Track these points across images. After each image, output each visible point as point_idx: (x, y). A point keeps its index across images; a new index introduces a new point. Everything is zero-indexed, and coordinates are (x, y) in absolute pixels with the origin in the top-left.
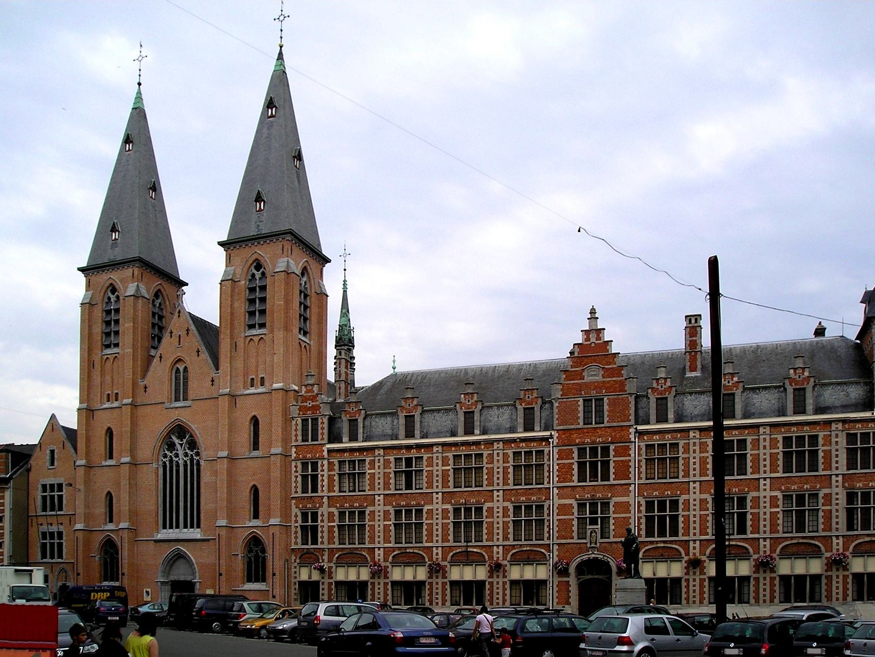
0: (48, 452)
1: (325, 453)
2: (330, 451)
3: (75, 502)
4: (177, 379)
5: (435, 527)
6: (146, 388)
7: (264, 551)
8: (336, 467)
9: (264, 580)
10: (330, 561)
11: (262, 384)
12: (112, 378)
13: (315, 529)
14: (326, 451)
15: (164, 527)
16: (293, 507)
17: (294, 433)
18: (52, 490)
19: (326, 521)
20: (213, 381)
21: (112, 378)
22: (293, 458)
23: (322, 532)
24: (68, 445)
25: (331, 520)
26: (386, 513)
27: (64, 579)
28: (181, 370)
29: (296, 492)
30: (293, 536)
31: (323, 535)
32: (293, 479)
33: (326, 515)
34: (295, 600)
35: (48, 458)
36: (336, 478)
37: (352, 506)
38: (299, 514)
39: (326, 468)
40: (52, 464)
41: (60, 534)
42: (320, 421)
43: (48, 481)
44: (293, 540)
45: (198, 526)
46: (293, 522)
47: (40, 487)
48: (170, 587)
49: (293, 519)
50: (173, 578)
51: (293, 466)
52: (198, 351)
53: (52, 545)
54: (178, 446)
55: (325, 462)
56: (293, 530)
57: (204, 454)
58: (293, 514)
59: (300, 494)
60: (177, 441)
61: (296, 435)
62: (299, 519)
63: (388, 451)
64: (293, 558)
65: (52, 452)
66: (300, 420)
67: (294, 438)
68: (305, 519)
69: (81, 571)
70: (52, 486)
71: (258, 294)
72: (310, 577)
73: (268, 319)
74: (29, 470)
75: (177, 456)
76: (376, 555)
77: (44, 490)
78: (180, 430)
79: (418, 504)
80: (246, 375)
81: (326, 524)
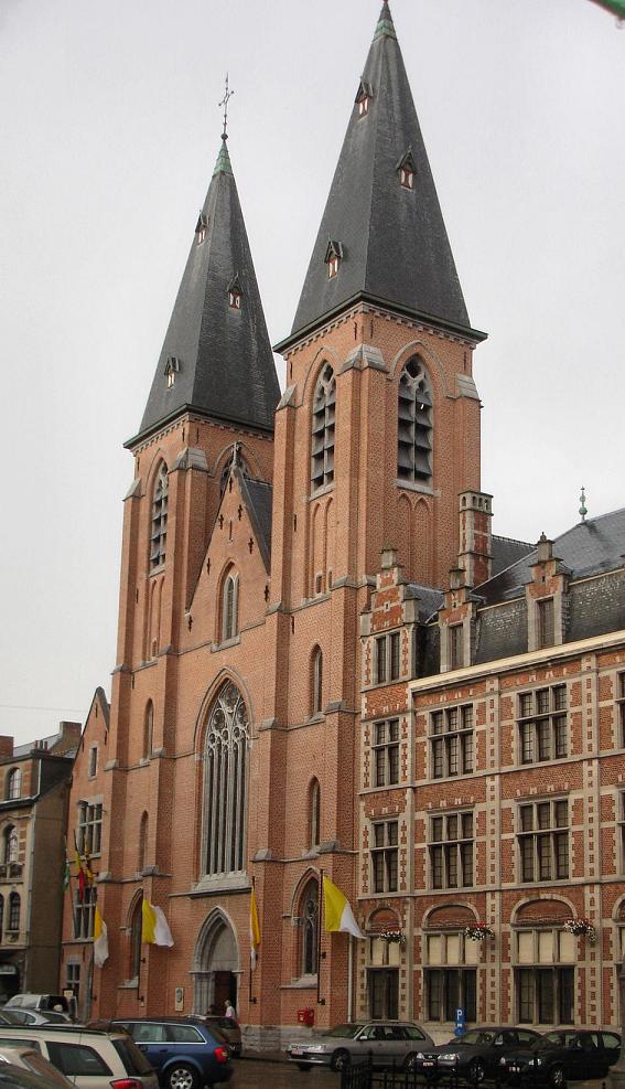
0: (91, 751)
2: (415, 695)
5: (587, 840)
6: (191, 622)
8: (428, 727)
10: (417, 924)
13: (392, 853)
14: (410, 696)
20: (267, 592)
22: (363, 717)
25: (418, 837)
26: (505, 813)
31: (405, 868)
34: (362, 1008)
36: (428, 749)
37: (451, 806)
38: (371, 829)
40: (94, 773)
48: (212, 985)
50: (215, 966)
55: (409, 718)
56: (361, 861)
58: (362, 829)
59: (371, 789)
60: (226, 709)
62: (371, 839)
63: (508, 680)
65: (95, 750)
68: (378, 841)
72: (387, 959)
74: (70, 786)
76: (489, 907)
79: (560, 791)
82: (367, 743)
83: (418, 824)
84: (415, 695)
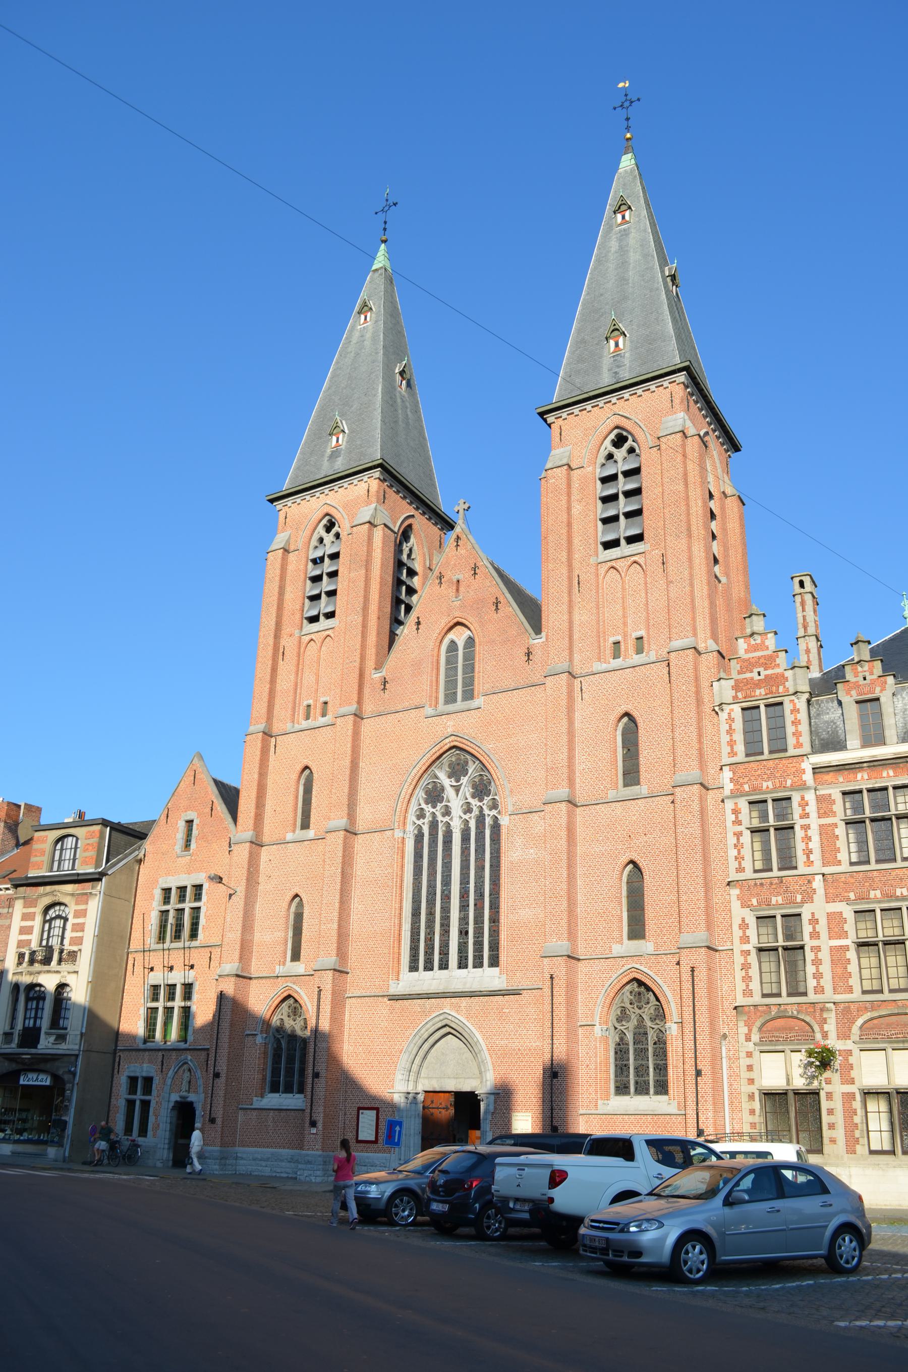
0: (182, 825)
1: (808, 777)
2: (816, 770)
3: (218, 916)
4: (451, 661)
6: (385, 682)
7: (660, 1015)
9: (662, 1088)
11: (639, 650)
12: (317, 675)
14: (809, 772)
15: (413, 968)
16: (736, 905)
17: (725, 738)
18: (182, 899)
19: (824, 934)
20: (528, 654)
21: (317, 675)
22: (727, 792)
23: (817, 962)
24: (221, 808)
27: (185, 1086)
28: (461, 644)
29: (740, 869)
30: (739, 974)
32: (732, 840)
33: (823, 921)
35: (181, 835)
39: (812, 808)
40: (187, 845)
41: (188, 988)
42: (788, 707)
43: (173, 882)
44: (740, 986)
45: (494, 962)
46: (737, 941)
47: (158, 894)
49: (737, 933)
51: (728, 812)
52: (497, 604)
53: (169, 1011)
54: (450, 792)
55: (810, 796)
57: (508, 802)
58: (736, 922)
60: (447, 782)
61: (732, 743)
64: (743, 1030)
65: (190, 822)
66: (737, 708)
67: (726, 749)
69: (222, 1067)
70: (182, 889)
71: (623, 485)
73: (649, 523)
75: (447, 812)
77: (166, 900)
78: (457, 757)
80: (600, 635)
81: (826, 943)
82: (738, 822)
83: (835, 920)
84: (816, 770)
